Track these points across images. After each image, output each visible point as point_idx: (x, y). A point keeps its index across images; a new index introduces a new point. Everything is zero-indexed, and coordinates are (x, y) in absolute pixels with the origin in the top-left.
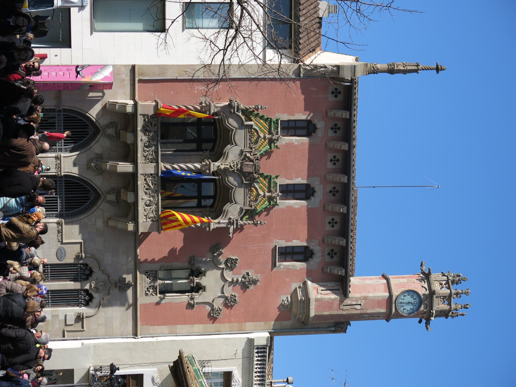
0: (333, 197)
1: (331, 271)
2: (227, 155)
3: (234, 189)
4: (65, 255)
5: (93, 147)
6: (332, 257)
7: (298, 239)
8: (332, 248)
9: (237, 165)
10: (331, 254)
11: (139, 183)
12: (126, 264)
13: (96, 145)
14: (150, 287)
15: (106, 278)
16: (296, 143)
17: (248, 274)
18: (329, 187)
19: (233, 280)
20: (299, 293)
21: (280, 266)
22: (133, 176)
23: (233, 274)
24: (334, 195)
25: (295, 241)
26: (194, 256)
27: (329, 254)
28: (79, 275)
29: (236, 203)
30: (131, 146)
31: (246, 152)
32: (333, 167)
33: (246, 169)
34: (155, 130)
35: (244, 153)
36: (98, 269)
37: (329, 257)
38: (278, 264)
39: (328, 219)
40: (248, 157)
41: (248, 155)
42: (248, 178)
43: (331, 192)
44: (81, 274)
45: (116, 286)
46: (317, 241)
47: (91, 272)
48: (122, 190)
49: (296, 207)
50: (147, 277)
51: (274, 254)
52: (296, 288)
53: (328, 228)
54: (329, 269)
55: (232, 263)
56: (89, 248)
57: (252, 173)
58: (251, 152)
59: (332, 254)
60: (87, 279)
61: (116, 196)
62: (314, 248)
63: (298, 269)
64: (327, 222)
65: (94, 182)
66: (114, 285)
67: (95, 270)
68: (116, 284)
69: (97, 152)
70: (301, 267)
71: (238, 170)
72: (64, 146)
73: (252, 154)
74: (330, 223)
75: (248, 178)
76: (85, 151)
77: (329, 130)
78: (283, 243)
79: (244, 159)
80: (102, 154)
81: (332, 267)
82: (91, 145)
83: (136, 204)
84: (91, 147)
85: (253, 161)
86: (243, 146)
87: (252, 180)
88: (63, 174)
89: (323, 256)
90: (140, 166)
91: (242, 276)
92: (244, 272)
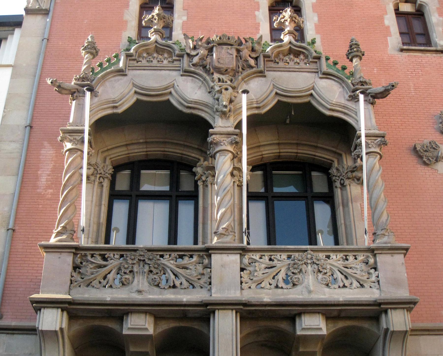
2: (196, 103)
7: (381, 19)
11: (267, 299)
16: (185, 18)
22: (248, 313)
25: (387, 22)
29: (313, 88)
30: (165, 326)
34: (117, 256)
35: (192, 69)
40: (202, 59)
42: (252, 62)
49: (316, 19)
51: (419, 54)
57: (238, 51)
58: (188, 55)
70: (436, 15)
71: (231, 81)
73: (193, 53)
78: (394, 39)
79: (204, 67)
83: (330, 311)
85: (211, 50)
86: (174, 73)
87: (254, 55)
90: (217, 295)
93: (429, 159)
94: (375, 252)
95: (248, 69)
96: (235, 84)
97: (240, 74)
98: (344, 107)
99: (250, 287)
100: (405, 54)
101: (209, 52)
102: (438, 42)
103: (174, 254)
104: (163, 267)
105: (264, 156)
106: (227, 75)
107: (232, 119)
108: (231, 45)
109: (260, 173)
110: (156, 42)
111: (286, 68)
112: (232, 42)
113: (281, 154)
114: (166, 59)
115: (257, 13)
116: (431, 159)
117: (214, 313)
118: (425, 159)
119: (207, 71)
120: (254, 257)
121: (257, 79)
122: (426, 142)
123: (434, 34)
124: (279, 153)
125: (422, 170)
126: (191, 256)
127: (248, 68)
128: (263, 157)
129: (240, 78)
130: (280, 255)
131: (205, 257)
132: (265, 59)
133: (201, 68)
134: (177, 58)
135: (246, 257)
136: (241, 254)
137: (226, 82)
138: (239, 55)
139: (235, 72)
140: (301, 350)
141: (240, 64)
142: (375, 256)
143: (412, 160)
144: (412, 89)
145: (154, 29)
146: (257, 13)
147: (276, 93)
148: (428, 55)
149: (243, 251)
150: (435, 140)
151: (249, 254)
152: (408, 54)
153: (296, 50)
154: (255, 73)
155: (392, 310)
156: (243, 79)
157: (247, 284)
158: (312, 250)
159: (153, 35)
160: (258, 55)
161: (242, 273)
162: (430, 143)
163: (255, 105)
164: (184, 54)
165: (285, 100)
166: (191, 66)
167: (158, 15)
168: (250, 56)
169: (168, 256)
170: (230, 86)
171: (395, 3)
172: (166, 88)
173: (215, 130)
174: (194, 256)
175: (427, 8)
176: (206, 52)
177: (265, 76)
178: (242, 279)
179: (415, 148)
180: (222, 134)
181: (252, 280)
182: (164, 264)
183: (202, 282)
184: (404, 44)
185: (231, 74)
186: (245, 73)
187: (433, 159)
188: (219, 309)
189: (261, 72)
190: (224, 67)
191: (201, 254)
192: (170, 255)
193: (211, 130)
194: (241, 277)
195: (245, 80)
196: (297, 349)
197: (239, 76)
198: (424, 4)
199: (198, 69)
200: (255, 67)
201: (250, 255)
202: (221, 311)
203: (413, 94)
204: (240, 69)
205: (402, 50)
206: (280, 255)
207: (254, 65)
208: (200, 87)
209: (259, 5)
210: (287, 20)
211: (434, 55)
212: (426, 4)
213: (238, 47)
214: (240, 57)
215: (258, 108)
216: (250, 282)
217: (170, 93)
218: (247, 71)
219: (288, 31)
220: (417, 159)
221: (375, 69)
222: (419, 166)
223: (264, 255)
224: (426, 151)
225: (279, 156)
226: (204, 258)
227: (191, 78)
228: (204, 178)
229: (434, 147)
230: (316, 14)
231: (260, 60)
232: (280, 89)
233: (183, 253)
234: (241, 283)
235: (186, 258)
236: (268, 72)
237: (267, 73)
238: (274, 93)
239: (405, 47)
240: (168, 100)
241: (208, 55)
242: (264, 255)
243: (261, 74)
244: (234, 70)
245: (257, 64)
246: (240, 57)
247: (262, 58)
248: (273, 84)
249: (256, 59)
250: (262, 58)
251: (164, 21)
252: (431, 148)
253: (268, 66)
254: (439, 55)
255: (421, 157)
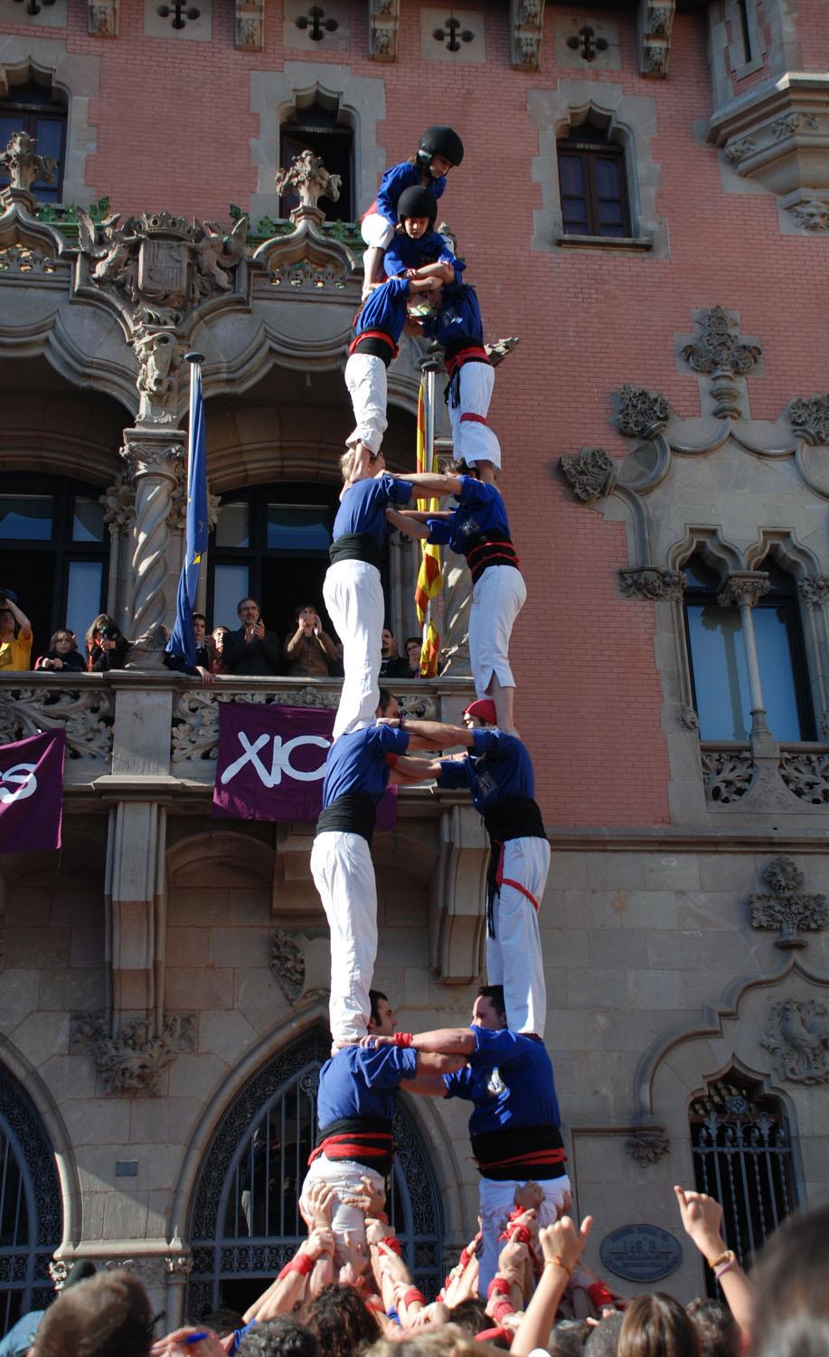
0: (339, 30)
1: (659, 33)
2: (100, 367)
3: (275, 346)
4: (646, 1229)
5: (35, 1061)
6: (602, 45)
8: (561, 42)
9: (151, 319)
10: (588, 48)
12: (683, 893)
13: (22, 1046)
14: (787, 781)
15: (757, 1003)
16: (92, 147)
17: (689, 352)
18: (300, 40)
19: (719, 414)
20: (766, 145)
21: (651, 233)
23: (697, 414)
24: (332, 26)
26: (621, 574)
27: (588, 56)
28: (755, 1150)
31: (86, 279)
32: (205, 19)
33: (174, 272)
35: (95, 289)
36: (714, 1043)
37: (601, 56)
38: (643, 240)
39: (439, 50)
40: (113, 268)
41: (100, 269)
42: (223, 279)
43: (316, 36)
44: (747, 1139)
45: (800, 946)
46: (534, 94)
47: (734, 1079)
48: (279, 903)
50: (740, 792)
51: (597, 252)
52: (745, 174)
53: (474, 53)
54: (656, 44)
55: (643, 413)
56: (605, 1091)
57: (194, 253)
59: (587, 42)
60: (772, 1105)
61: (311, 938)
62: (564, 105)
63: (659, 166)
64: (449, 55)
65: (232, 1058)
66: (796, 956)
67: (718, 1056)
68: (786, 947)
69: (63, 1039)
71: (176, 320)
72: (23, 1241)
74: (453, 47)
75: (223, 279)
76: (54, 1108)
77: (37, 20)
78: (548, 214)
79: (121, 286)
80: (77, 1016)
81: (646, 28)
82: (20, 1073)
84: (33, 1073)
85: (134, 249)
87: (228, 263)
88: (176, 1244)
89: (597, 76)
91: (704, 381)
92: (683, 371)
93: (586, 491)
94: (439, 693)
95: (215, 294)
96: (184, 329)
97: (196, 304)
98: (409, 383)
99: (189, 758)
100: (566, 252)
101: (130, 252)
102: (642, 223)
103: (41, 692)
104: (17, 716)
105: (250, 473)
106: (168, 309)
107: (174, 404)
108: (180, 239)
109: (241, 505)
110: (17, 220)
111: (295, 293)
112: (181, 232)
113: (286, 470)
114: (38, 262)
115: (253, 142)
116: (591, 491)
117: (115, 807)
118: (578, 491)
119: (125, 296)
120: (201, 698)
121: (232, 317)
122: (587, 450)
123: (637, 203)
124: (282, 467)
125: (570, 510)
126: (76, 696)
127: (216, 290)
128: (247, 475)
129: (195, 314)
130: (253, 695)
131: (104, 696)
132: (253, 272)
133: (114, 288)
134: (63, 262)
135: (184, 697)
136: (174, 691)
137: (165, 323)
138: (195, 266)
139: (186, 303)
140: (287, 878)
141: (198, 282)
142: (439, 698)
143: (552, 492)
144: (571, 334)
145: (12, 189)
146: (253, 142)
147: (271, 350)
148: (617, 253)
149: (179, 688)
150: (604, 447)
151: (192, 692)
152: (573, 251)
153: (320, 252)
154: (227, 303)
155: (463, 809)
156: (201, 317)
157: (184, 752)
158: (314, 687)
159: (10, 204)
160: (237, 263)
161: (174, 729)
162: (593, 454)
163: (224, 376)
164: (77, 254)
165: (288, 364)
166: (92, 281)
167: (19, 156)
168: (218, 264)
169: (29, 694)
170: (173, 333)
171: (560, 124)
172: (38, 331)
173: (138, 429)
174: (81, 694)
175: (631, 137)
176: (125, 255)
177: (249, 312)
178: (175, 741)
179: (560, 466)
180: (150, 440)
181: (194, 742)
182: (19, 710)
183: (94, 746)
184: (568, 224)
185: (176, 304)
186: (207, 304)
187: (595, 489)
188: (124, 802)
189: (240, 302)
190: (162, 288)
191: (96, 690)
192: (33, 692)
193: (128, 430)
194: (173, 738)
195: (206, 318)
196: (282, 875)
197: (193, 309)
198: (625, 128)
199: (106, 291)
200: (229, 290)
201: (193, 694)
202: (129, 807)
203: (572, 344)
204: (197, 294)
205: (560, 243)
206: (253, 695)
207: (227, 286)
208: (110, 332)
209: (258, 121)
210: (303, 182)
211: (630, 254)
212: (630, 129)
213: (193, 244)
214: (198, 266)
215: (229, 382)
216: (190, 746)
217: (47, 341)
218: (213, 297)
219: (304, 207)
220: (563, 488)
221: (498, 286)
222: (566, 504)
223: (221, 694)
224: (582, 473)
225: (282, 473)
226: (102, 699)
227: (91, 309)
228: (120, 520)
229: (599, 461)
230: (383, 151)
231: (240, 274)
232: (279, 341)
233: (59, 688)
234: (173, 748)
235: (65, 699)
236: (256, 302)
237: (253, 304)
238: (264, 350)
239: (567, 237)
240: (42, 357)
241: (128, 259)
242: (221, 694)
243: (242, 305)
244: (183, 296)
245: (233, 282)
246: (198, 266)
247: (244, 270)
248: (266, 330)
249: (232, 271)
250: (244, 270)
251: (35, 170)
252: (593, 466)
253: (257, 287)
254: (639, 255)
255: (571, 486)
